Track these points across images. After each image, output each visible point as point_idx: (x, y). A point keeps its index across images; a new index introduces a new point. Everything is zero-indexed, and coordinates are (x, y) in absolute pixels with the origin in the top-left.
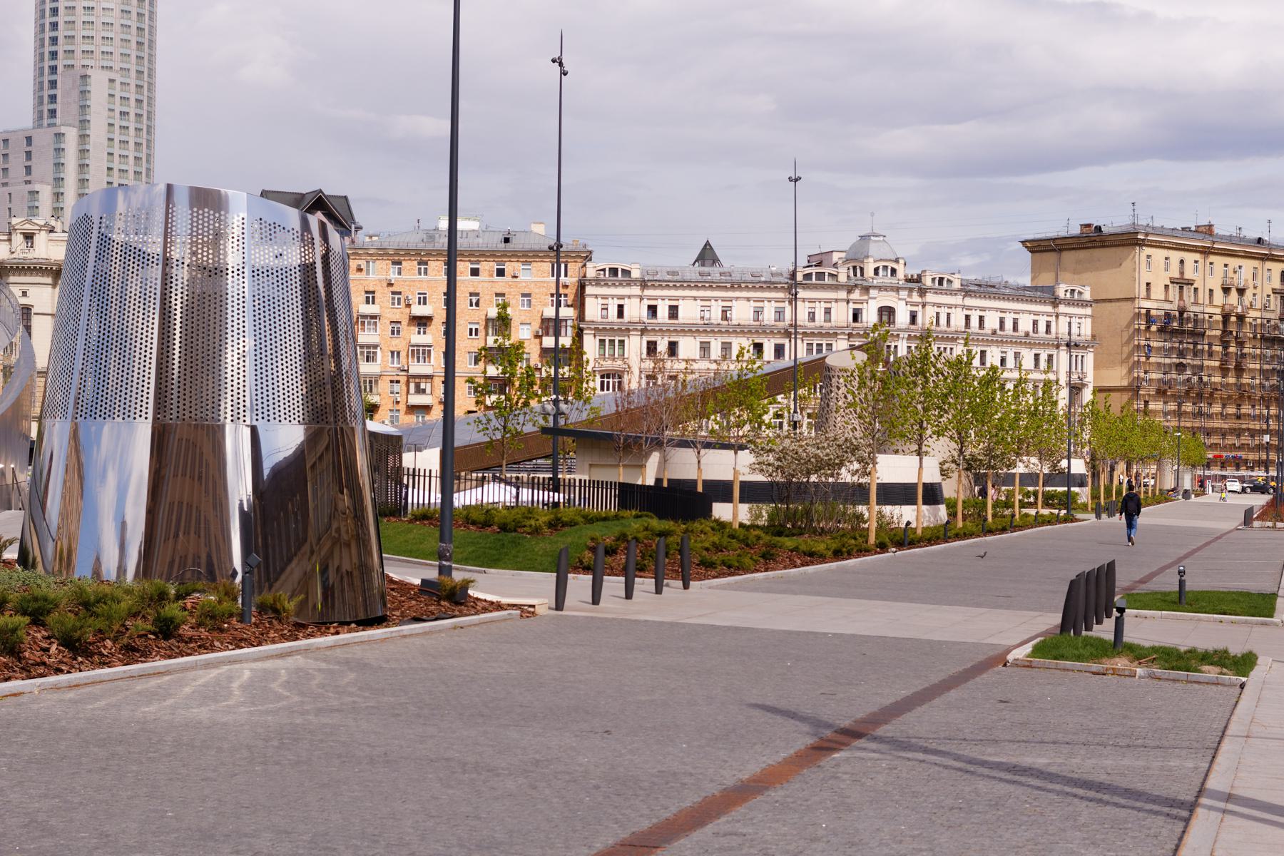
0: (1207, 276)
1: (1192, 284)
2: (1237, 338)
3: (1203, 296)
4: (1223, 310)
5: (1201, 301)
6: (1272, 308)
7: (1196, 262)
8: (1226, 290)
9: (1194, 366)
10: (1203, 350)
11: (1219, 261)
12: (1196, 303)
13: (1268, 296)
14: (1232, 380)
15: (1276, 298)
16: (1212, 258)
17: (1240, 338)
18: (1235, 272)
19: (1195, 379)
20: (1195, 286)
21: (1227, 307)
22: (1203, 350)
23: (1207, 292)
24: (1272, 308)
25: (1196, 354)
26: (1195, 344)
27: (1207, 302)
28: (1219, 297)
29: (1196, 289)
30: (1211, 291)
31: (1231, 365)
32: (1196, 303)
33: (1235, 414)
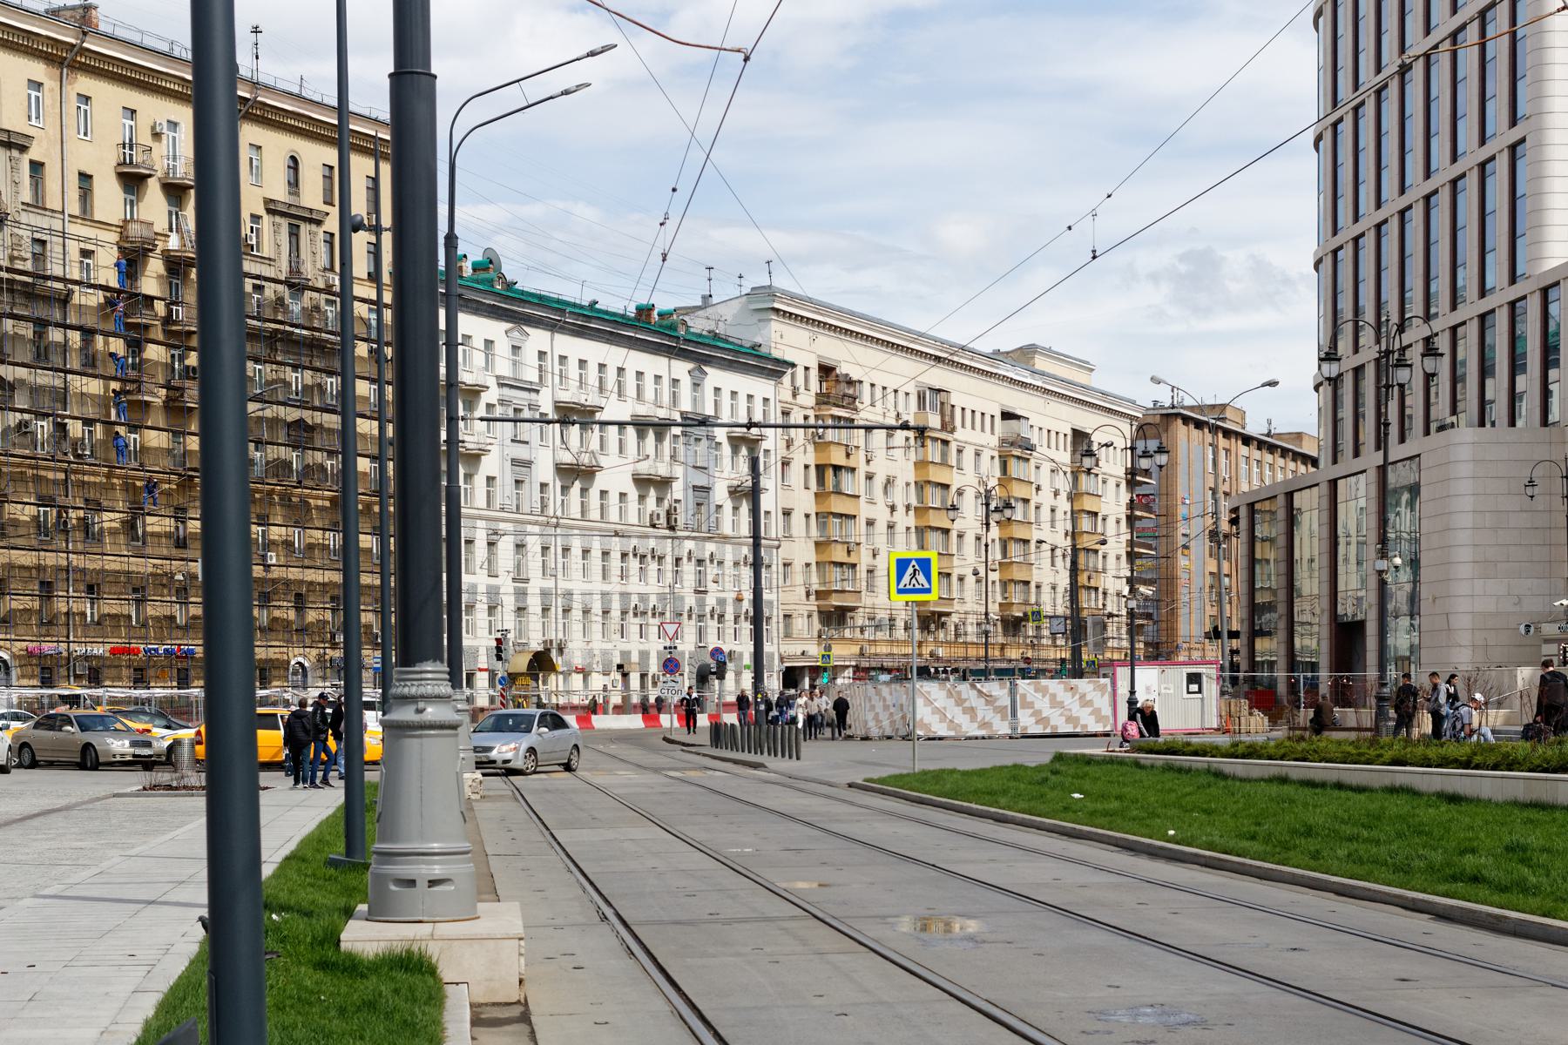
0: (70, 131)
1: (23, 149)
2: (168, 320)
3: (60, 191)
4: (124, 237)
5: (53, 202)
6: (267, 251)
7: (38, 86)
8: (132, 181)
9: (35, 391)
10: (65, 347)
11: (108, 97)
12: (38, 205)
13: (256, 218)
14: (156, 439)
15: (276, 228)
16: (85, 84)
17: (176, 323)
18: (157, 136)
19: (43, 428)
20: (35, 153)
21: (134, 230)
22: (65, 347)
23: (73, 182)
24: (267, 251)
25: (42, 355)
26: (41, 324)
27: (74, 207)
28: (109, 199)
29: (36, 166)
30: (85, 177)
31: (152, 393)
32: (38, 205)
33: (168, 535)
